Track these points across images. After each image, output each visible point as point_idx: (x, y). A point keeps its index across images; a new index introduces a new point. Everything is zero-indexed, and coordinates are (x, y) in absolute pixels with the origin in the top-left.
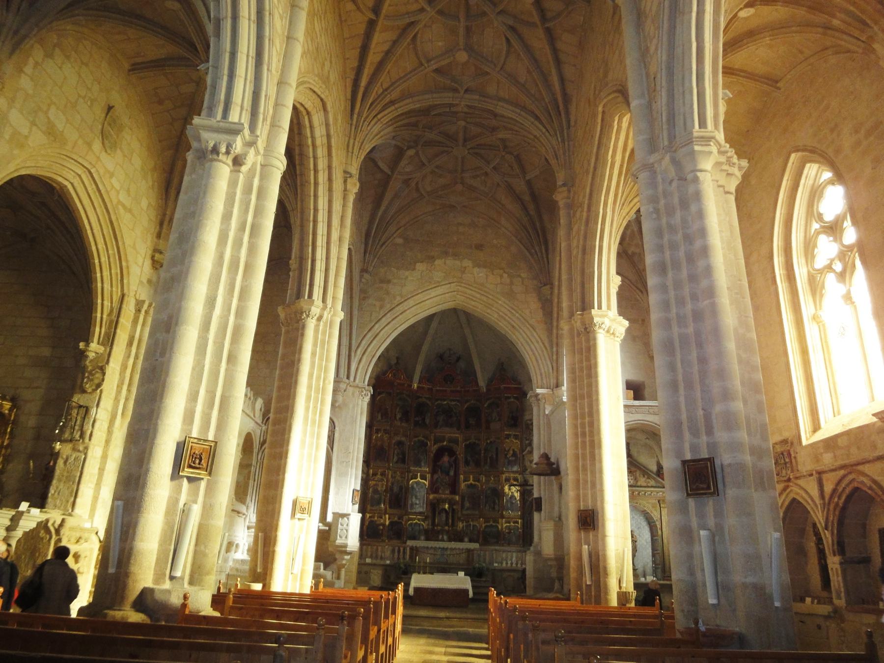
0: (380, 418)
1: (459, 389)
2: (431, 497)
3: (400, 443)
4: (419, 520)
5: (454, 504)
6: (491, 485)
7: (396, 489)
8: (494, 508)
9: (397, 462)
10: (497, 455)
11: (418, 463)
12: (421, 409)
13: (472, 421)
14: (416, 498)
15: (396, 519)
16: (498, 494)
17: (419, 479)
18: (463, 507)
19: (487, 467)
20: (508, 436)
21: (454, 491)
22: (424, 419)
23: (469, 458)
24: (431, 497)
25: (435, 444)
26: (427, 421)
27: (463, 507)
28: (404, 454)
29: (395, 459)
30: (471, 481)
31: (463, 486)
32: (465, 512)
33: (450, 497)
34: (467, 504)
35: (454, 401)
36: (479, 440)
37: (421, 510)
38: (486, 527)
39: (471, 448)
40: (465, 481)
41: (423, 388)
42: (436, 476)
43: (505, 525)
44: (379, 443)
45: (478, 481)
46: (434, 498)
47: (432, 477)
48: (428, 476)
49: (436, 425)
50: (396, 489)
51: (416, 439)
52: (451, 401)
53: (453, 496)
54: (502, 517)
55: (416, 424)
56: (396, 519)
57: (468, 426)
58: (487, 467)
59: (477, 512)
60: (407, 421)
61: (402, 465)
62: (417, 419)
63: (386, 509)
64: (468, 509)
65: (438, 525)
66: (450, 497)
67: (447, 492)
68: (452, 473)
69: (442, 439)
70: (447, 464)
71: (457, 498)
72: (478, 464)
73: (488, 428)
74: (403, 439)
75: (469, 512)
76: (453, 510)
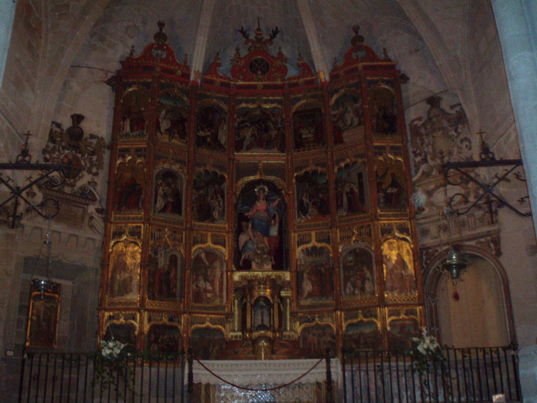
0: (128, 128)
1: (279, 82)
2: (237, 276)
3: (169, 175)
4: (213, 322)
5: (281, 288)
6: (353, 245)
7: (162, 262)
8: (363, 289)
9: (164, 210)
10: (361, 185)
11: (205, 213)
12: (208, 118)
13: (307, 134)
14: (206, 280)
15: (165, 320)
16: (366, 260)
17: (210, 244)
18: (299, 291)
19: (343, 213)
20: (380, 150)
21: (278, 266)
22: (215, 137)
23: (306, 200)
24: (237, 276)
25: (238, 179)
26: (223, 139)
27: (299, 291)
28: (177, 195)
29: (160, 204)
30: (314, 243)
31: (298, 252)
32: (302, 303)
33: (273, 274)
34: (308, 287)
35: (272, 102)
36: (323, 165)
37: (217, 302)
38: (350, 326)
39: (307, 180)
40: (300, 243)
41: (212, 82)
42: (243, 238)
43: (388, 320)
44: (128, 175)
45: (328, 241)
46: (243, 278)
47: (237, 240)
48: (229, 238)
49: (239, 146)
50: (162, 262)
51: (201, 169)
52: (266, 102)
53: (279, 273)
54: (382, 303)
55: (201, 142)
56: (165, 320)
57: (299, 144)
58: (343, 213)
59: (330, 301)
60: (183, 135)
61: (176, 217)
62: (201, 134)
63: (142, 300)
64: (310, 295)
65: (251, 331)
66: (273, 274)
67: (270, 267)
68: (274, 232)
69: (253, 169)
70: (263, 215)
71: (287, 276)
72: (323, 209)
73: (339, 140)
74: (176, 167)
75: (308, 302)
76: (282, 299)
